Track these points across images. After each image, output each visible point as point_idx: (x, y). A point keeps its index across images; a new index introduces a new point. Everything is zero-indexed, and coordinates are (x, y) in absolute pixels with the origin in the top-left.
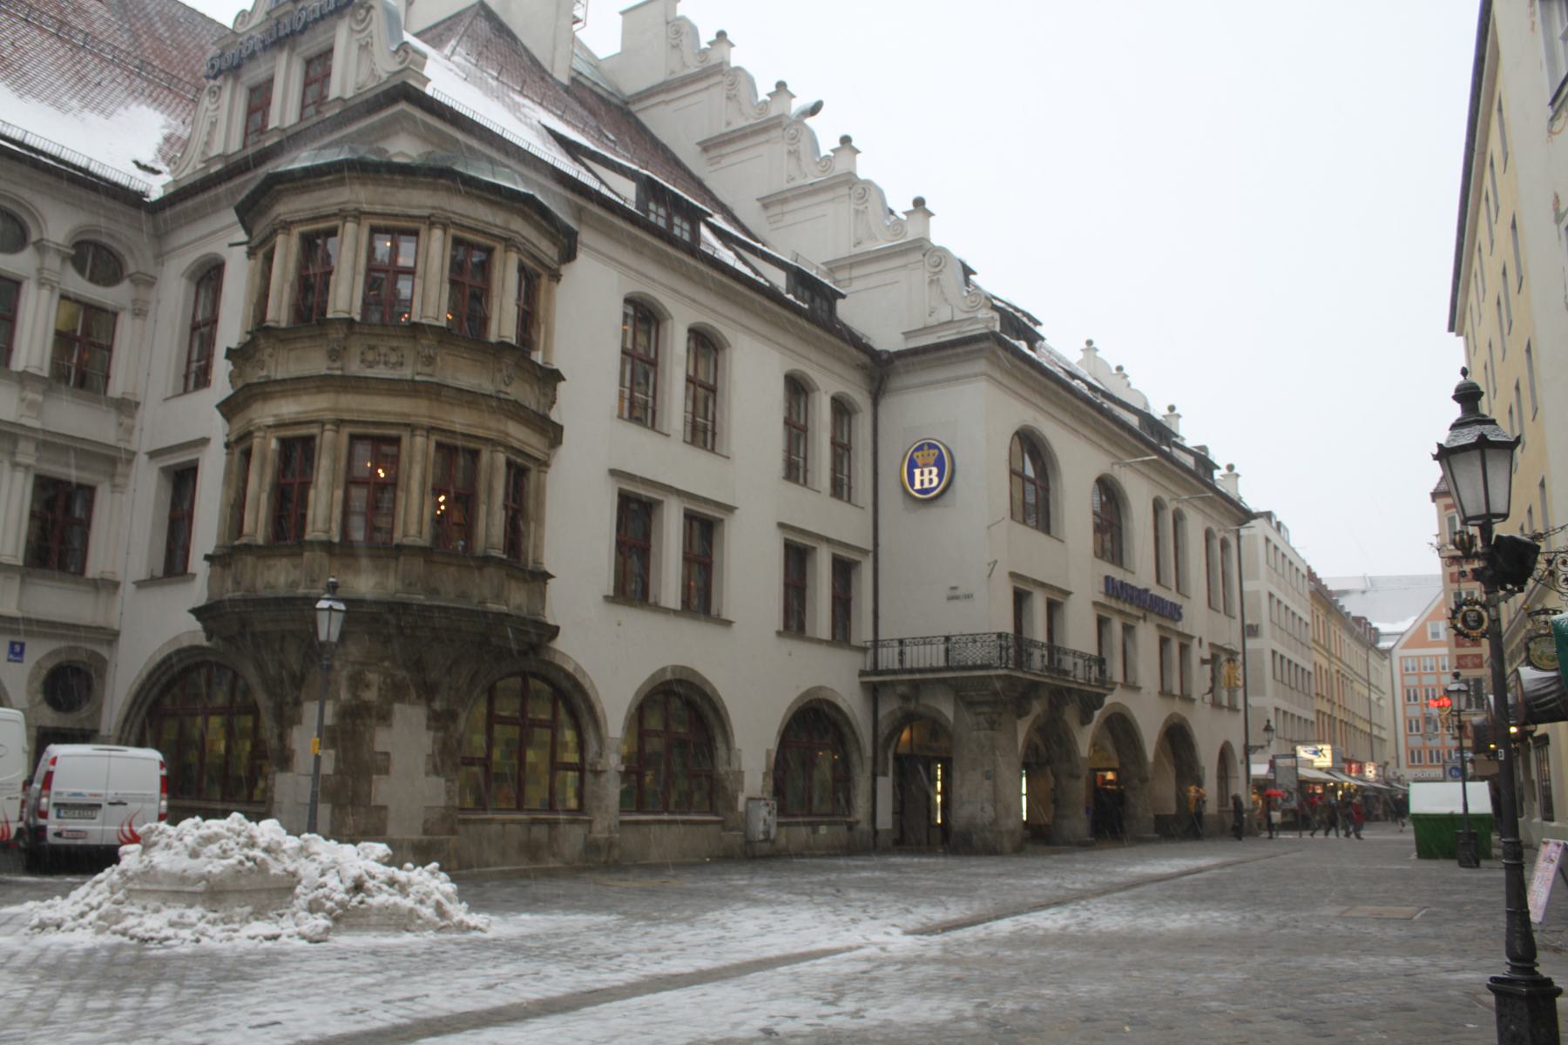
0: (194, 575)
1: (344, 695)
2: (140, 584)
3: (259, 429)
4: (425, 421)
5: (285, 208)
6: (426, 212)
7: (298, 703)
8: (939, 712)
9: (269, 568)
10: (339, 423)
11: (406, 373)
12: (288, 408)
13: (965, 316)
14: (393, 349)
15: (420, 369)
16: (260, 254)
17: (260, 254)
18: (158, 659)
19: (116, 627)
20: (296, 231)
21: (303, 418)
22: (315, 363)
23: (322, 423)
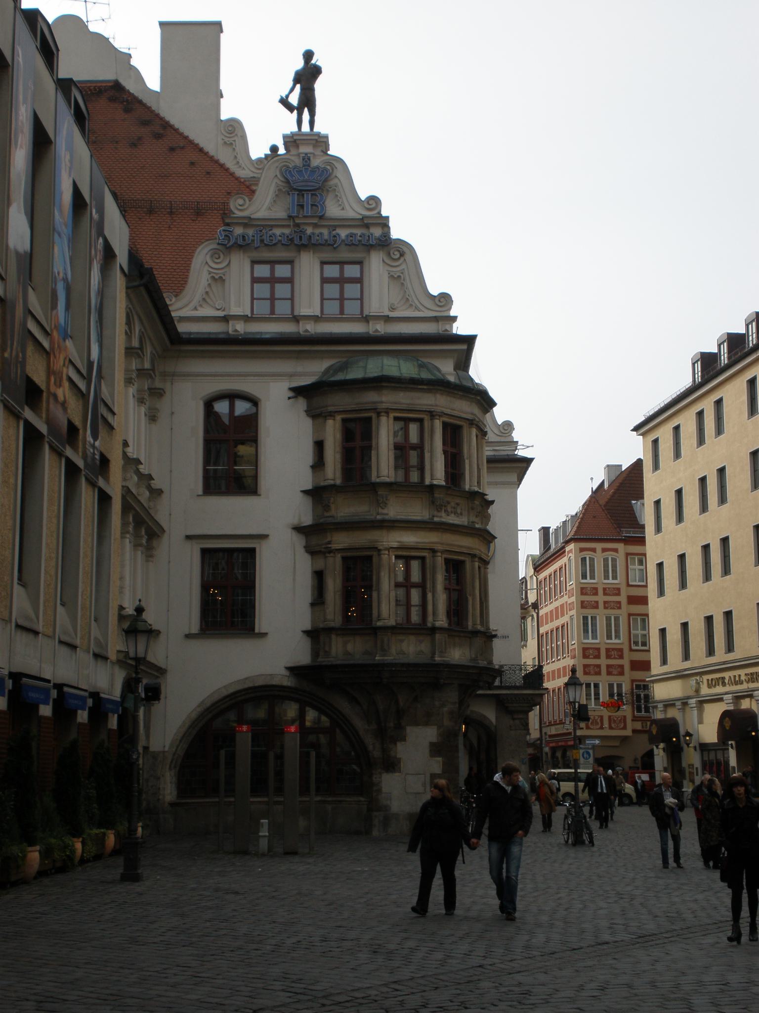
0: (263, 635)
1: (447, 722)
2: (188, 636)
3: (386, 549)
4: (477, 552)
5: (388, 398)
6: (469, 417)
7: (400, 727)
8: (485, 717)
9: (402, 641)
10: (443, 552)
11: (463, 520)
12: (409, 538)
13: (498, 439)
14: (458, 504)
15: (473, 519)
16: (339, 418)
17: (339, 418)
18: (225, 693)
19: (164, 667)
20: (392, 415)
21: (420, 546)
22: (417, 511)
23: (433, 551)
